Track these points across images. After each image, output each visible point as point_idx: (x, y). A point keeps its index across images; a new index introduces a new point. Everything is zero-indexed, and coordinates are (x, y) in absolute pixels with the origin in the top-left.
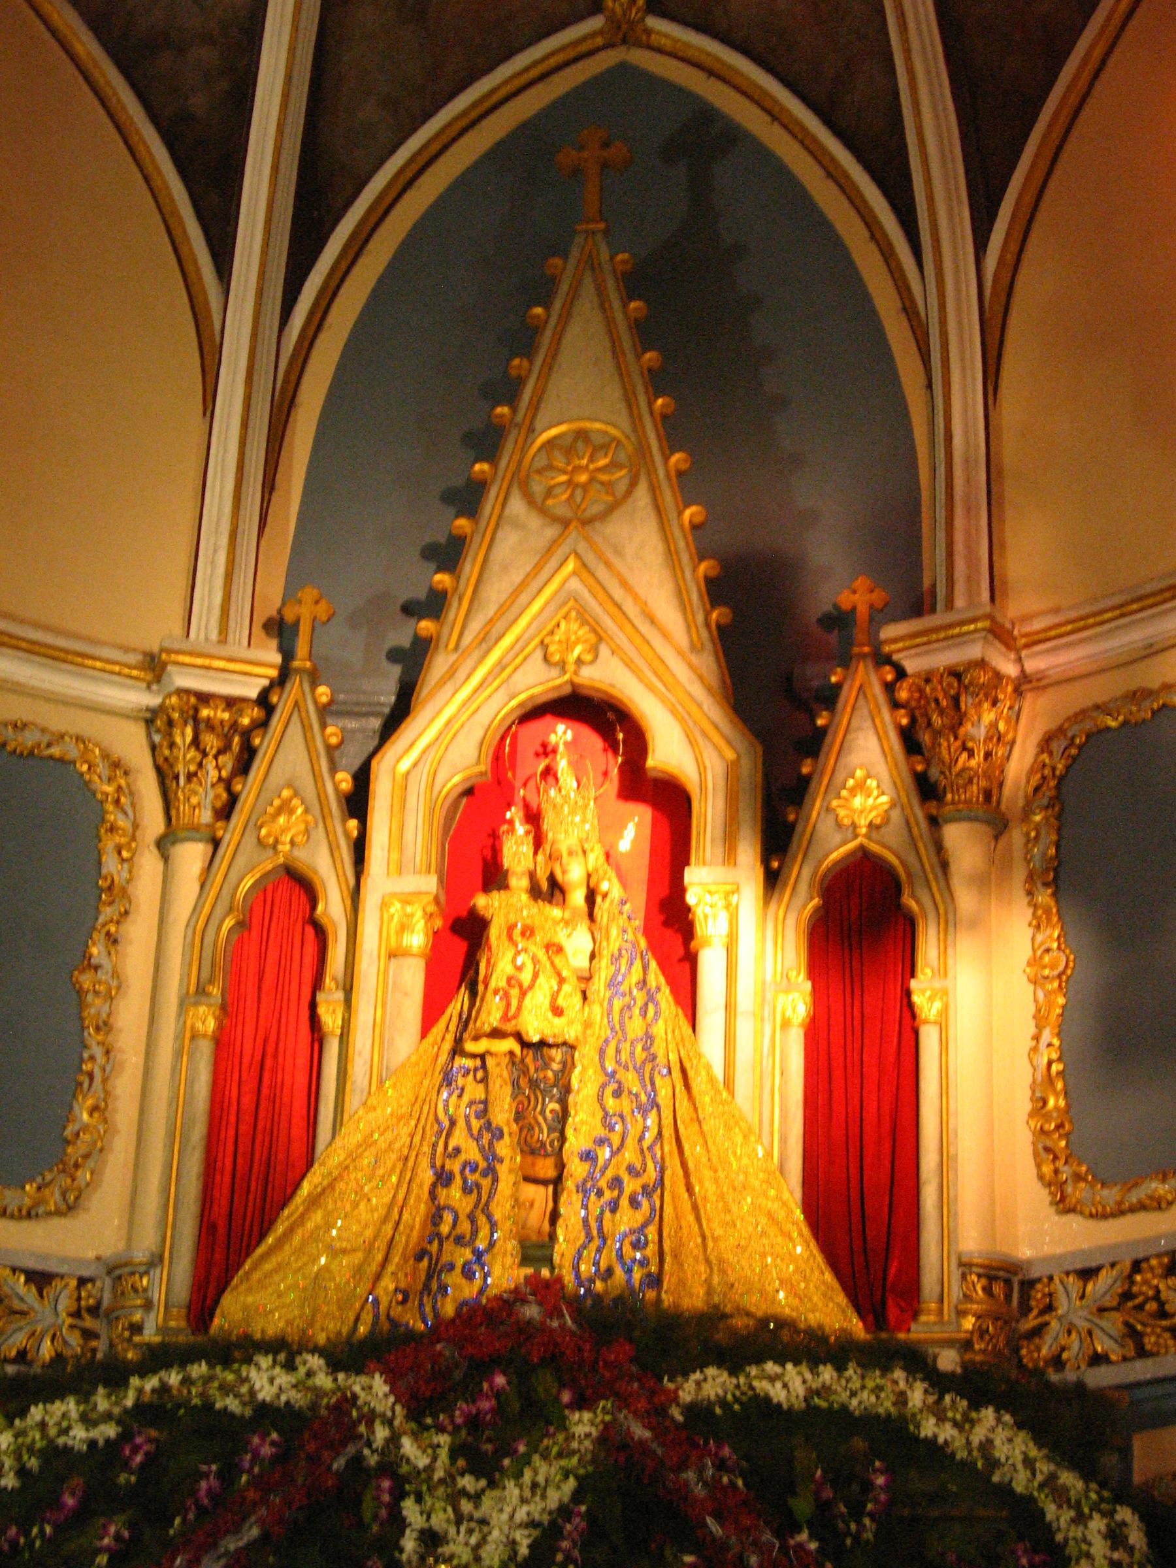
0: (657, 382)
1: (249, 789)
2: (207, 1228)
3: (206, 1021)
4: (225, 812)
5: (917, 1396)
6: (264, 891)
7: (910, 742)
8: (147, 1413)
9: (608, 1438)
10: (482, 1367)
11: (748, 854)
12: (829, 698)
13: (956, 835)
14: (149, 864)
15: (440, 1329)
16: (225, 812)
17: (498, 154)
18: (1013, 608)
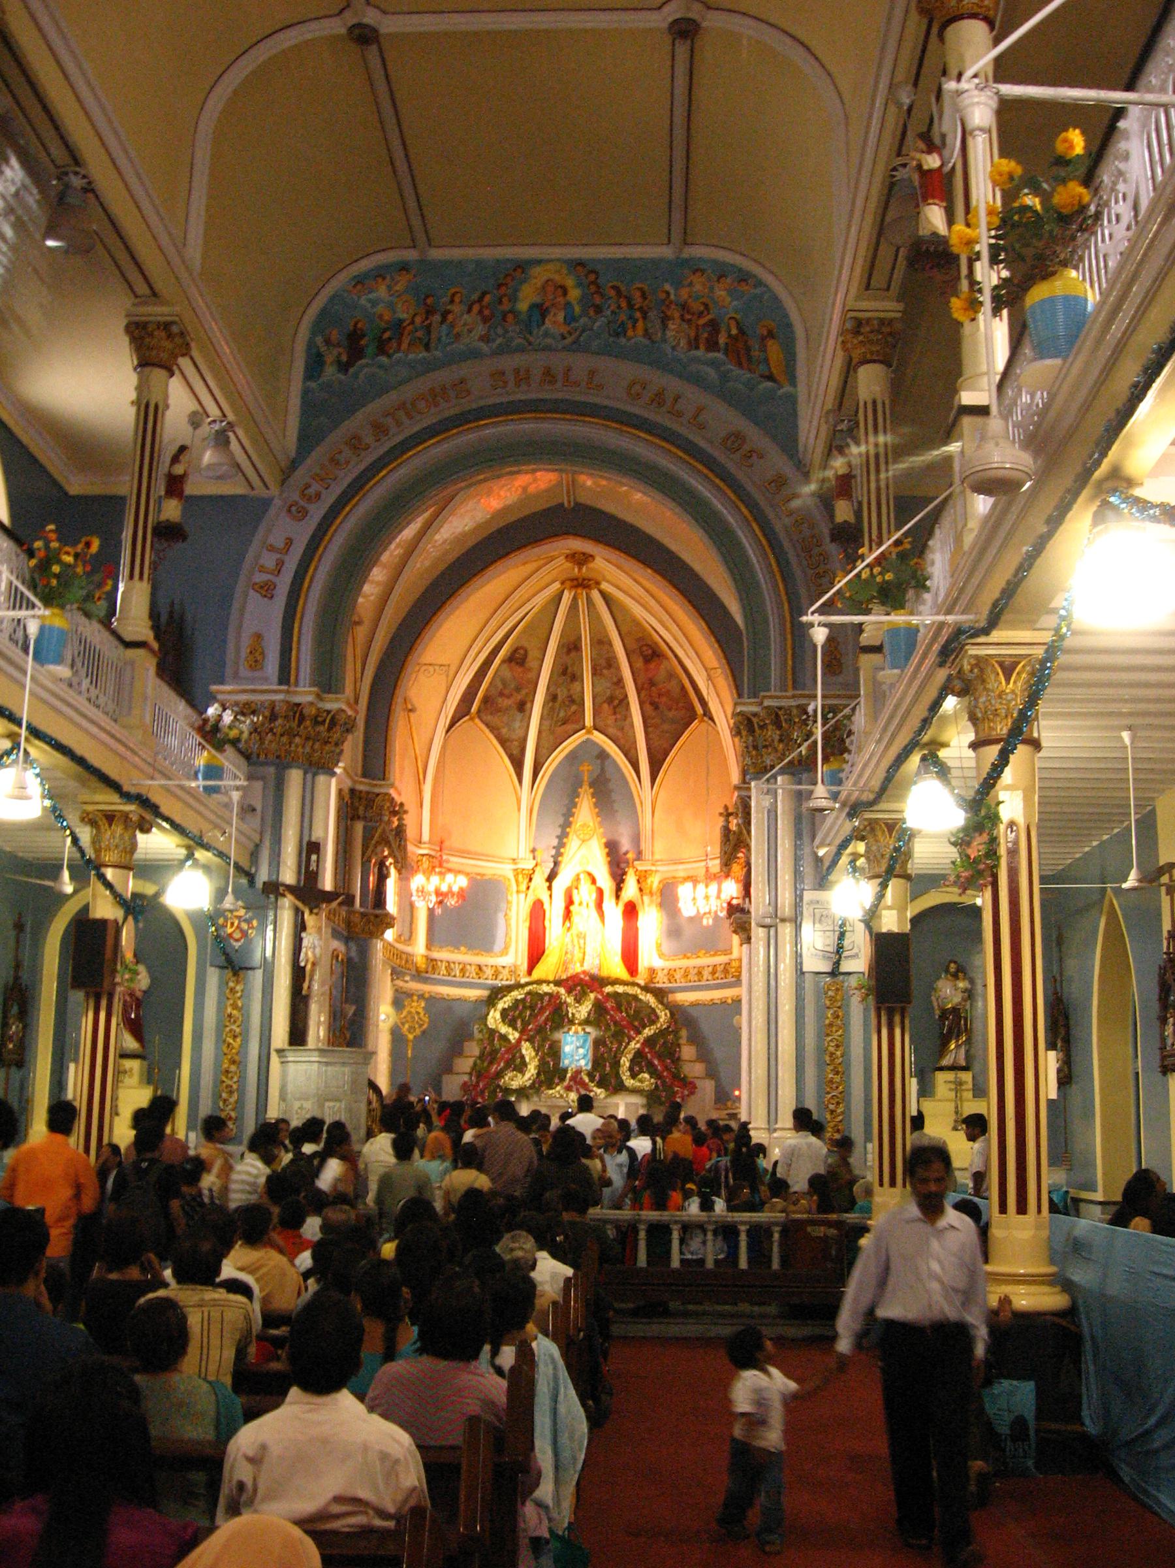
0: (598, 815)
1: (532, 885)
2: (529, 958)
3: (527, 924)
4: (528, 888)
5: (639, 991)
6: (534, 904)
7: (638, 881)
8: (529, 993)
9: (596, 999)
10: (576, 985)
11: (613, 900)
12: (625, 873)
13: (645, 898)
14: (515, 895)
15: (567, 979)
16: (528, 888)
17: (567, 757)
18: (657, 857)
